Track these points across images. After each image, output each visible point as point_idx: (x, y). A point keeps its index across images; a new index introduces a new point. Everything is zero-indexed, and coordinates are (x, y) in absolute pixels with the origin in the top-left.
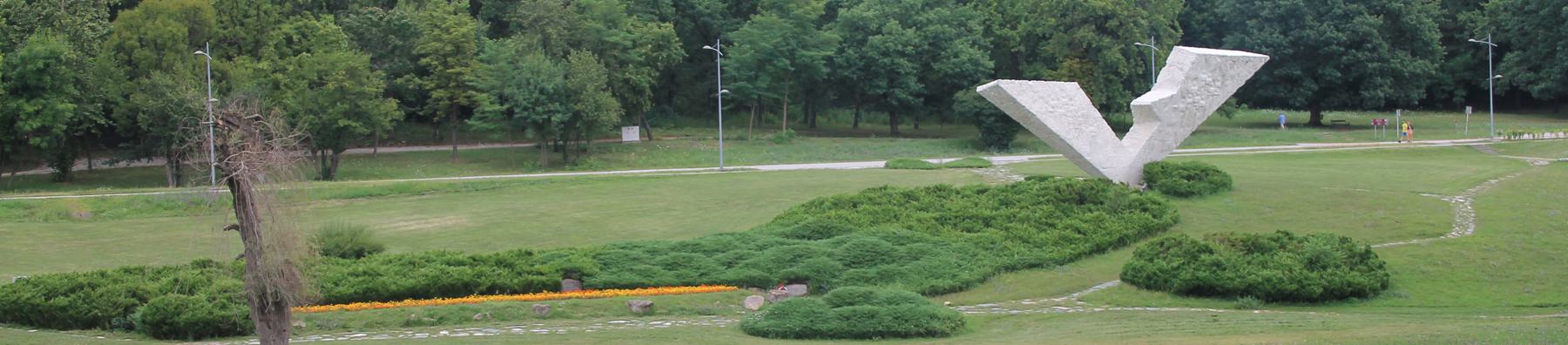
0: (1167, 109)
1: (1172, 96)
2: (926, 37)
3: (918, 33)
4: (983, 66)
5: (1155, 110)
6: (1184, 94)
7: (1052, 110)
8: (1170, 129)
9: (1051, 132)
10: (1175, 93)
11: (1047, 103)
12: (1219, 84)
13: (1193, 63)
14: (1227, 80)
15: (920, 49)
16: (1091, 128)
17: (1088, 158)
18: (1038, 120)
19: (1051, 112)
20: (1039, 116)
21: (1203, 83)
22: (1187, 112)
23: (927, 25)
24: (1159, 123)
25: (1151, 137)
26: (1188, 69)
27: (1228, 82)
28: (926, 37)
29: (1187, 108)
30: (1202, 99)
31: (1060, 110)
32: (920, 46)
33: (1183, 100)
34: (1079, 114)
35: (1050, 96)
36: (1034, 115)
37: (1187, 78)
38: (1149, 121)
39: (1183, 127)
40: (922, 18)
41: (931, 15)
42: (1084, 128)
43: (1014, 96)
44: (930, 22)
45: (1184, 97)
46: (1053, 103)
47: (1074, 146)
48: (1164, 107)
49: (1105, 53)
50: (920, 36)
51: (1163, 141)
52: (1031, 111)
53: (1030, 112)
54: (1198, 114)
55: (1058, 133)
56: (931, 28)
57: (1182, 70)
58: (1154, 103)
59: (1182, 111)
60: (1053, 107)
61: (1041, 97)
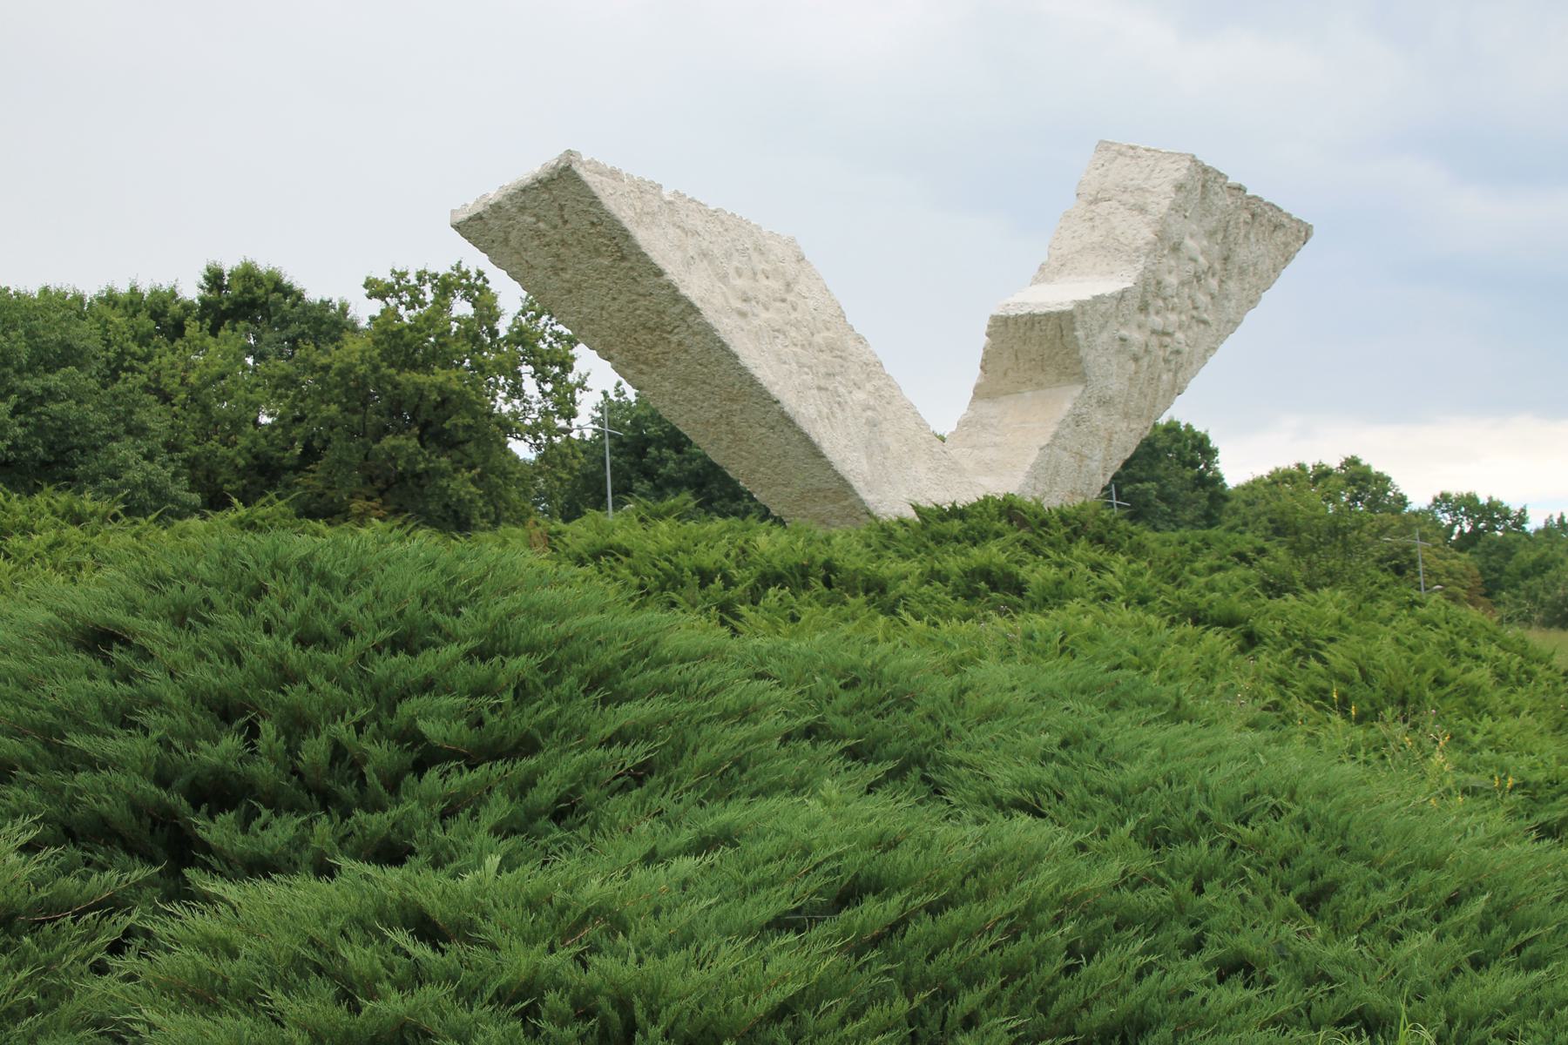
0: (1105, 336)
1: (1122, 296)
2: (40, 429)
3: (21, 417)
4: (174, 500)
5: (1080, 333)
6: (1148, 295)
7: (744, 307)
8: (1098, 416)
9: (750, 391)
10: (1130, 285)
11: (724, 278)
12: (1213, 283)
13: (1179, 187)
14: (1230, 278)
15: (25, 454)
16: (860, 396)
17: (869, 498)
18: (708, 330)
19: (743, 314)
20: (709, 315)
21: (1190, 267)
22: (1145, 362)
23: (41, 401)
24: (1081, 388)
25: (1056, 436)
26: (1167, 202)
27: (1232, 286)
28: (40, 429)
29: (1147, 351)
30: (1180, 327)
31: (765, 315)
32: (26, 448)
33: (1142, 317)
34: (818, 339)
35: (728, 255)
36: (692, 309)
37: (1161, 236)
38: (1040, 385)
39: (1126, 416)
40: (33, 384)
41: (54, 380)
42: (841, 390)
43: (626, 223)
44: (50, 394)
45: (1144, 308)
46: (739, 283)
47: (826, 447)
48: (1102, 327)
49: (444, 483)
50: (21, 425)
51: (1081, 457)
52: (683, 291)
53: (677, 298)
54: (1165, 377)
55: (775, 391)
56: (55, 408)
57: (1142, 210)
58: (1081, 305)
59: (1136, 359)
60: (745, 300)
61: (704, 255)
